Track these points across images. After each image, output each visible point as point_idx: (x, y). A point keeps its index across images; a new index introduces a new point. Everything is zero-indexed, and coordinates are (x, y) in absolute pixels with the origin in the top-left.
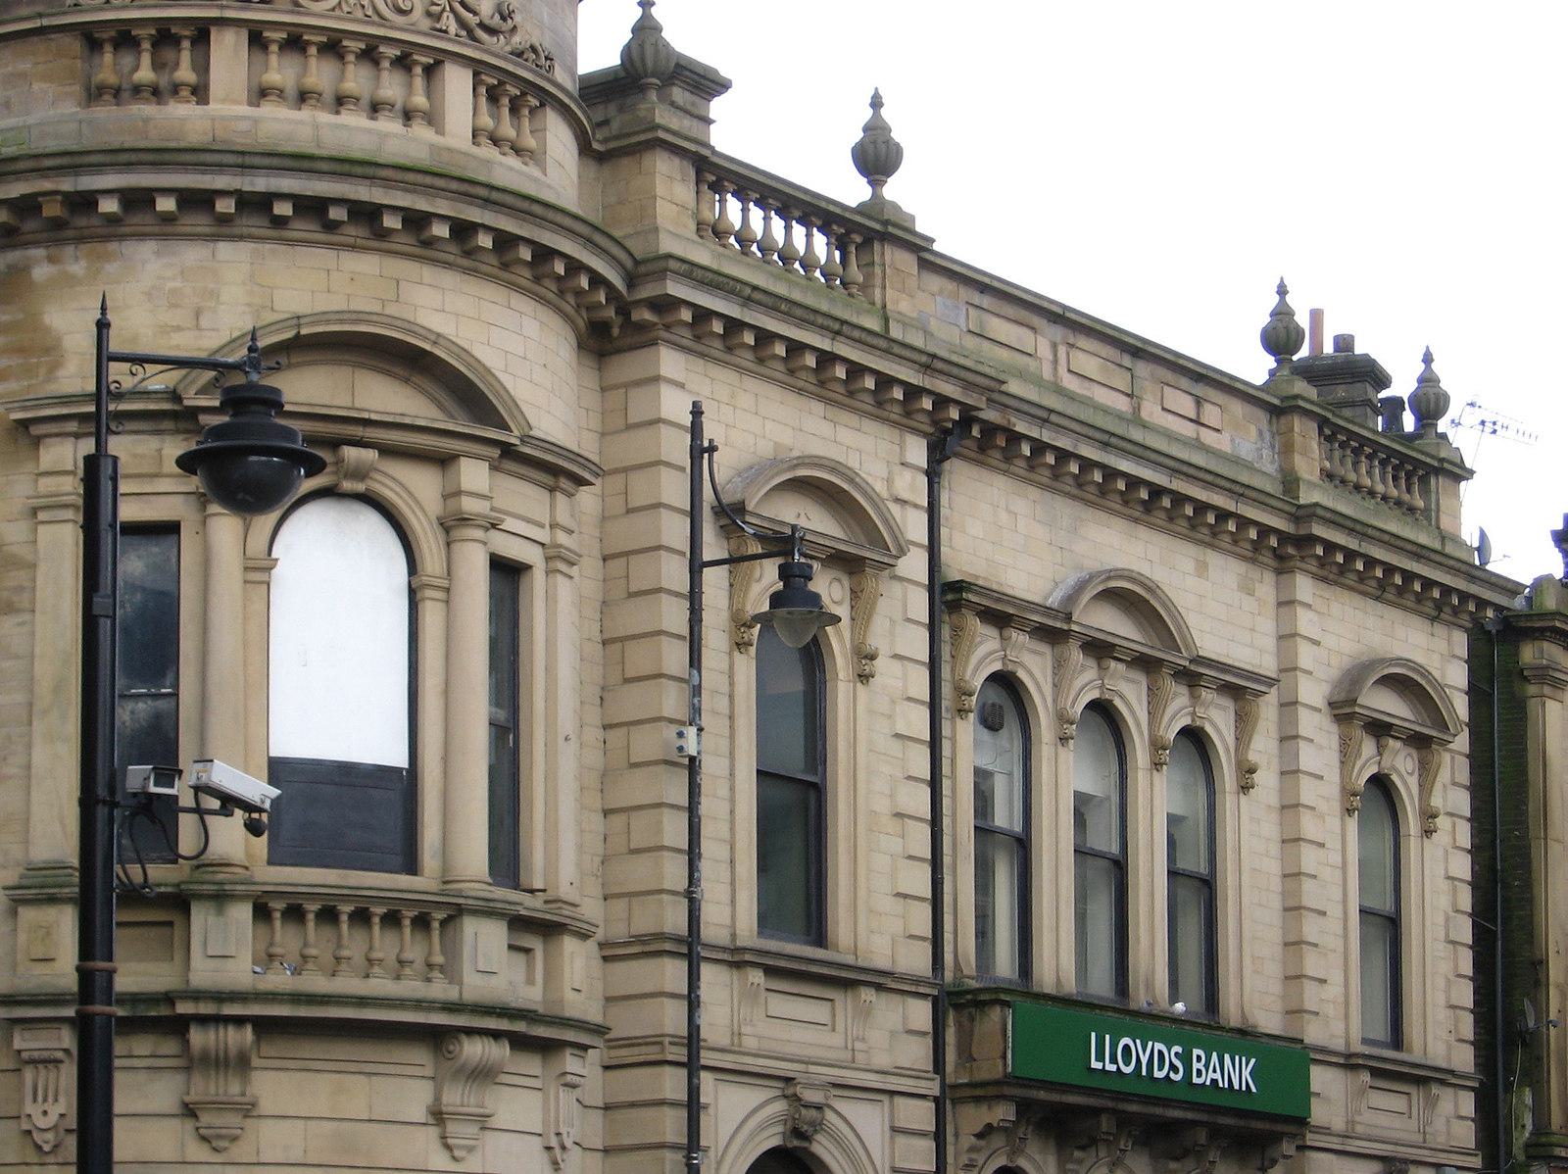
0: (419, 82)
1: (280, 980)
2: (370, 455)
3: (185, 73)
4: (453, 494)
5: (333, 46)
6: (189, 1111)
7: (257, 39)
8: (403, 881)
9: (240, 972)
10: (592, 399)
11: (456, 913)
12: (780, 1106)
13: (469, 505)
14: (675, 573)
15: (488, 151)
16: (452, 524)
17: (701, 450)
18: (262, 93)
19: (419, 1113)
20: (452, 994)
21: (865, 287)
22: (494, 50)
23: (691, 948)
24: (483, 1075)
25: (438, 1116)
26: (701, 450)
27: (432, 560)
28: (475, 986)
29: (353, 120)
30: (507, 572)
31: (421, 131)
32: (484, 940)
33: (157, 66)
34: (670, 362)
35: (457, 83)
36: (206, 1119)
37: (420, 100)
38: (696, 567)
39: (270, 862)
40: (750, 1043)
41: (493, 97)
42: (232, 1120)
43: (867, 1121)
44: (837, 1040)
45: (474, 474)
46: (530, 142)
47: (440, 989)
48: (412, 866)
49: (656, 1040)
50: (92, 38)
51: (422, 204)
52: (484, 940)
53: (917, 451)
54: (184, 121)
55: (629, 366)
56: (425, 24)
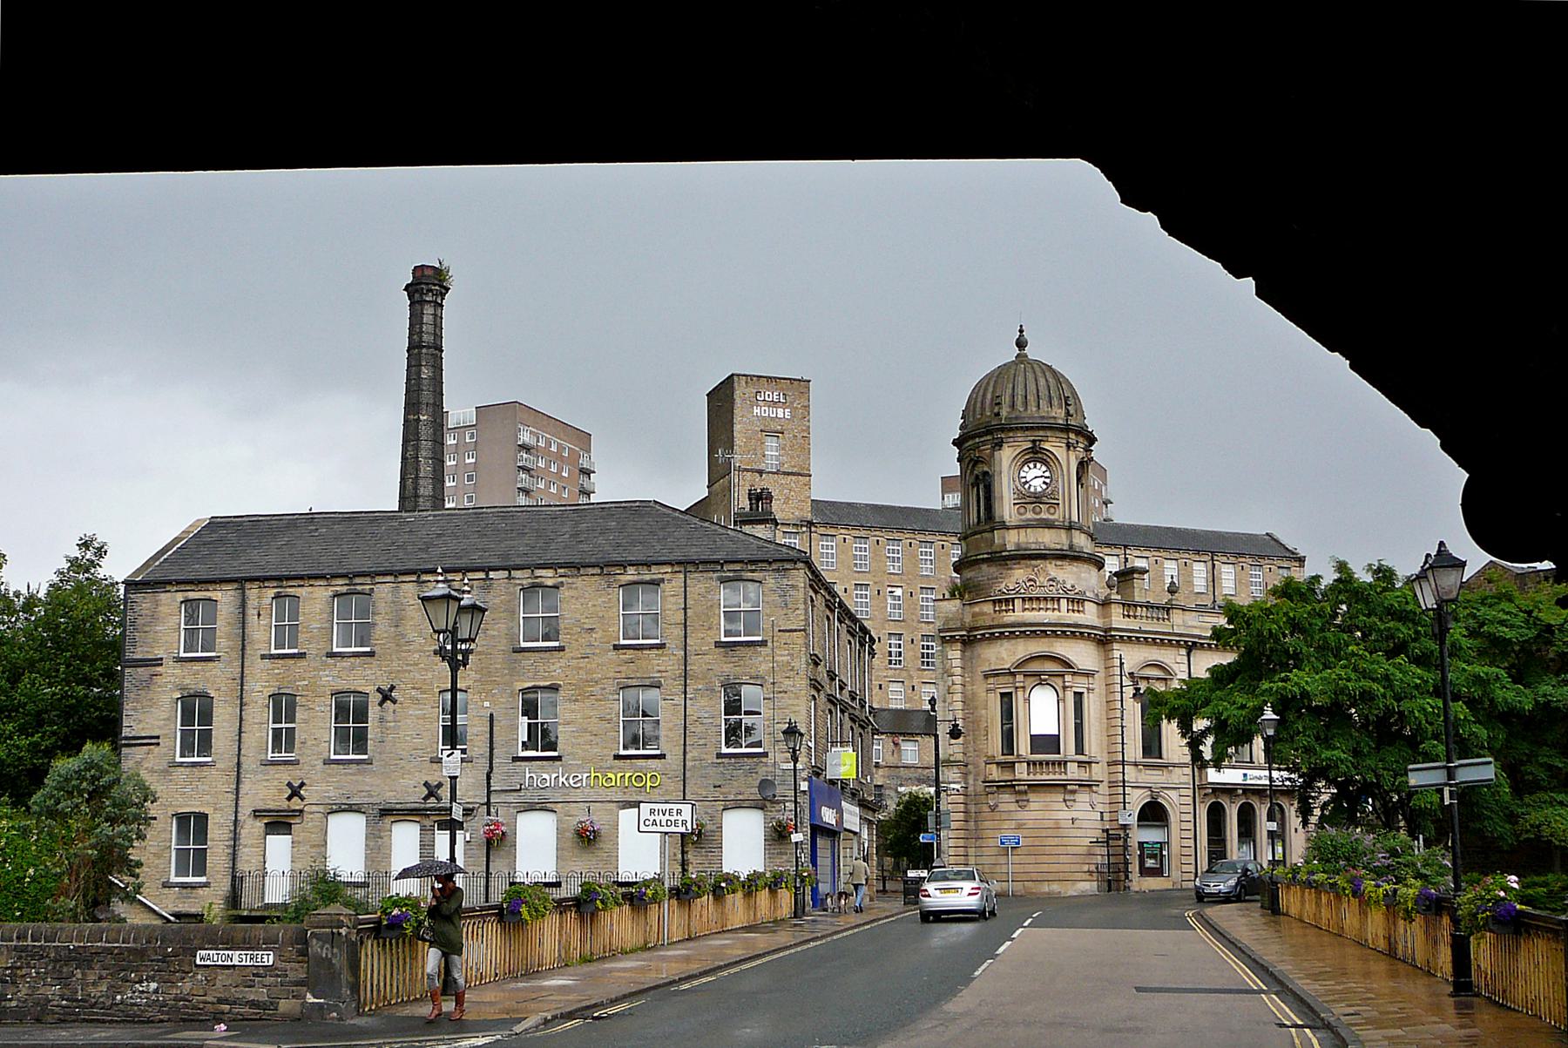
0: (1056, 602)
1: (1032, 777)
2: (1047, 677)
3: (1011, 607)
4: (1064, 682)
5: (1038, 599)
6: (1017, 802)
7: (1023, 599)
8: (1058, 756)
9: (1025, 776)
10: (1103, 654)
11: (1066, 762)
12: (1149, 793)
13: (1067, 684)
14: (1118, 688)
15: (1071, 613)
16: (1064, 688)
17: (1122, 664)
18: (1024, 610)
19: (1062, 800)
20: (1066, 778)
21: (1168, 619)
22: (1071, 595)
23: (1123, 763)
24: (1074, 792)
25: (1065, 801)
26: (1122, 664)
27: (1061, 695)
28: (1070, 776)
29: (1042, 612)
30: (1078, 696)
31: (1056, 612)
32: (1072, 767)
33: (1006, 605)
34: (1116, 646)
35: (1064, 602)
36: (1020, 803)
37: (1056, 607)
38: (1122, 687)
39: (1031, 754)
40: (1140, 781)
41: (1073, 602)
42: (1025, 803)
43: (1173, 794)
44: (1164, 778)
45: (1068, 678)
46: (1081, 609)
47: (1063, 777)
48: (1059, 753)
49: (1116, 782)
50: (994, 602)
51: (1054, 629)
52: (1072, 767)
53: (1183, 652)
54: (1010, 618)
55: (1108, 647)
56: (1056, 592)
